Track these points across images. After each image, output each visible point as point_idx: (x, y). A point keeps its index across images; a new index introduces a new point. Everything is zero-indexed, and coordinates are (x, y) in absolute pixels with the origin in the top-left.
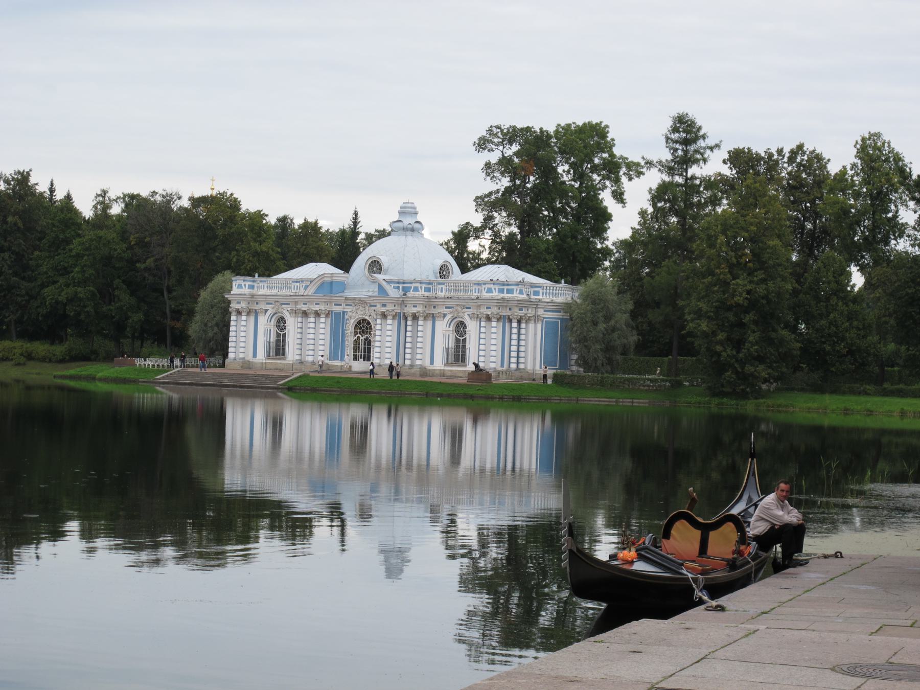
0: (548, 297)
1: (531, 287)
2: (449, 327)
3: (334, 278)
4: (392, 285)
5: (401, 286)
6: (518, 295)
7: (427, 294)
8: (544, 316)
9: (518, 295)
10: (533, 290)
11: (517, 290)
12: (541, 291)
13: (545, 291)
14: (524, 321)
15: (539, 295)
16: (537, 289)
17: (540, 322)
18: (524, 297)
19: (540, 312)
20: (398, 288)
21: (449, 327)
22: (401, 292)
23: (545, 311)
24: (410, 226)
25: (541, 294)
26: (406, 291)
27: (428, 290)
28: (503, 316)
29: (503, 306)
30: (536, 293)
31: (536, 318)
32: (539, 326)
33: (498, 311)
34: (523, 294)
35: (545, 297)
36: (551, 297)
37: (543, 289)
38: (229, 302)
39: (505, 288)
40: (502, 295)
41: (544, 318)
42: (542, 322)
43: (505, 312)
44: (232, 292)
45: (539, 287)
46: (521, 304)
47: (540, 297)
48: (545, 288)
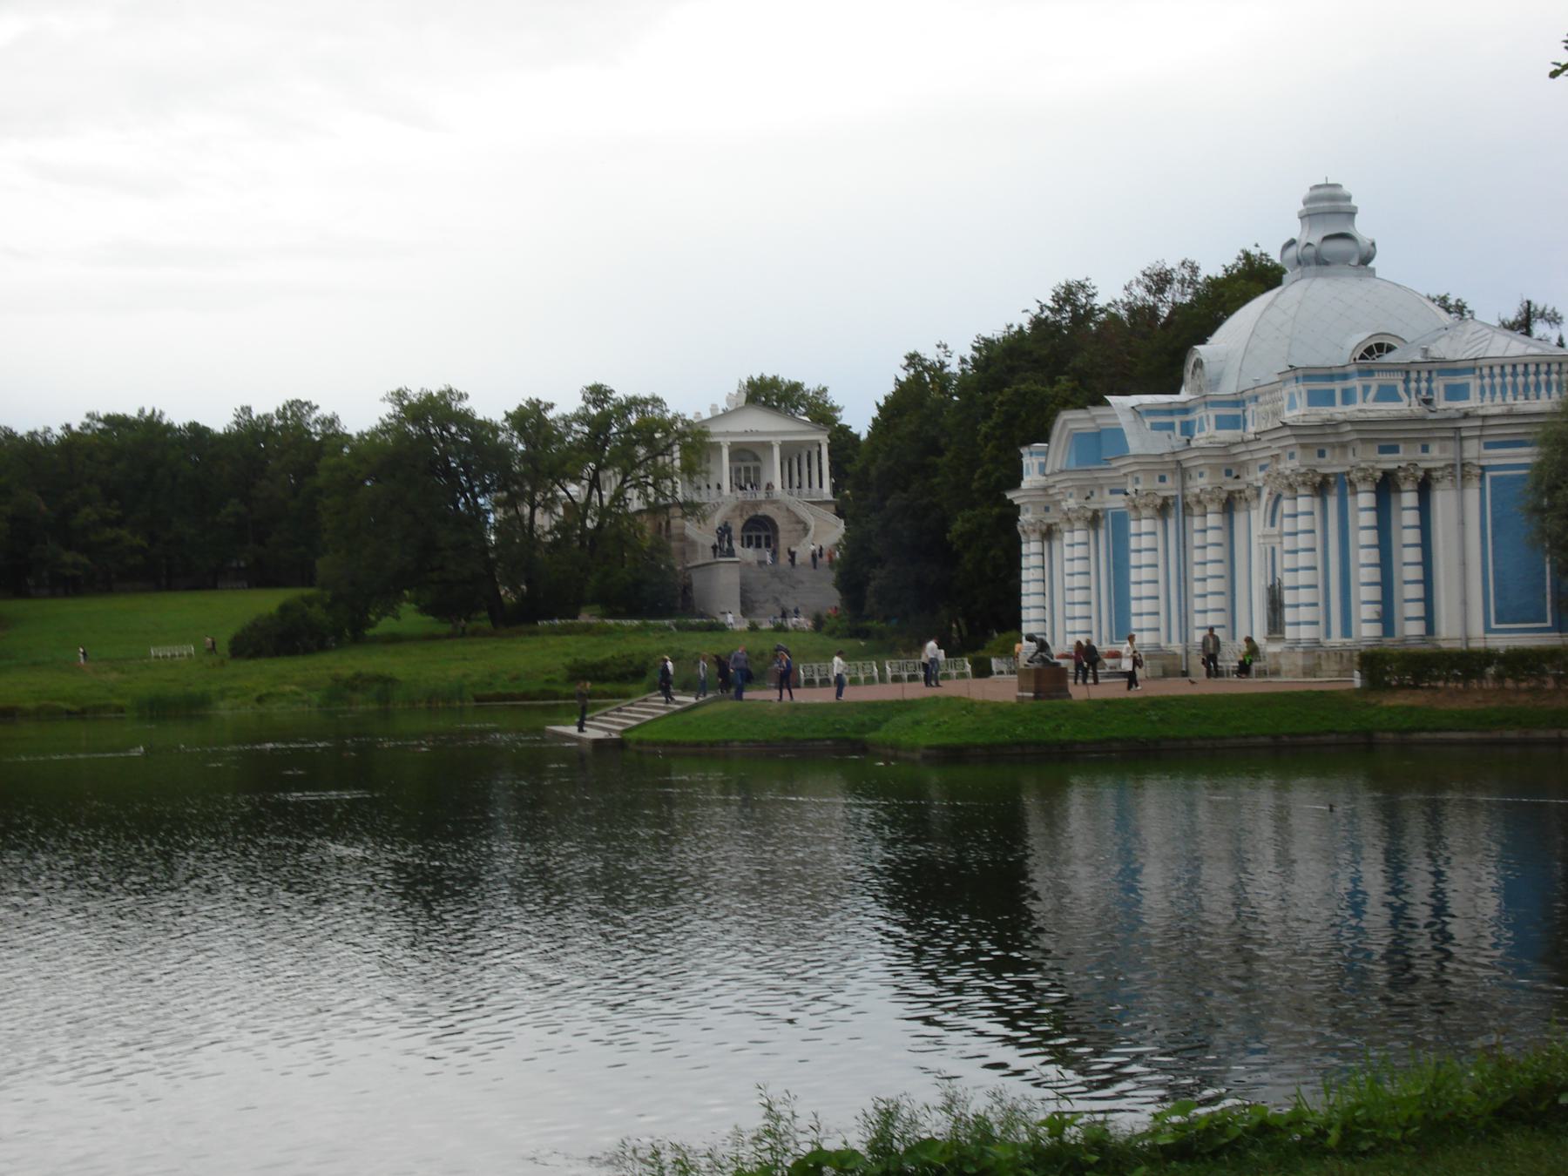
0: (1498, 400)
1: (1442, 372)
2: (1273, 524)
3: (1099, 421)
4: (1148, 421)
5: (1177, 420)
6: (1370, 405)
7: (1226, 435)
8: (1483, 463)
9: (1370, 405)
10: (1439, 384)
11: (1366, 389)
12: (1473, 382)
13: (1487, 381)
14: (1408, 486)
15: (1467, 398)
16: (1459, 380)
17: (1475, 483)
18: (1405, 406)
19: (1473, 450)
20: (1171, 426)
21: (1273, 524)
22: (1178, 438)
23: (1488, 446)
24: (1310, 250)
25: (1474, 392)
26: (1187, 429)
27: (1222, 423)
28: (1335, 474)
29: (1333, 446)
30: (1456, 393)
31: (1462, 472)
32: (1472, 495)
33: (1314, 460)
34: (1398, 399)
35: (1487, 402)
36: (1510, 400)
37: (1482, 377)
38: (1016, 510)
39: (1338, 386)
40: (1325, 412)
41: (1483, 468)
42: (1482, 478)
43: (1332, 464)
44: (1024, 485)
45: (1472, 370)
46: (1383, 435)
47: (1472, 403)
48: (1486, 371)
